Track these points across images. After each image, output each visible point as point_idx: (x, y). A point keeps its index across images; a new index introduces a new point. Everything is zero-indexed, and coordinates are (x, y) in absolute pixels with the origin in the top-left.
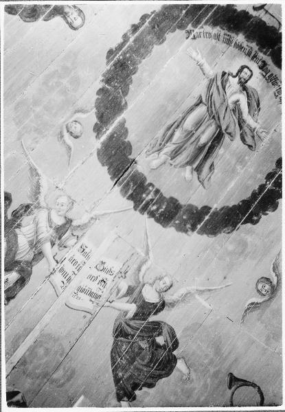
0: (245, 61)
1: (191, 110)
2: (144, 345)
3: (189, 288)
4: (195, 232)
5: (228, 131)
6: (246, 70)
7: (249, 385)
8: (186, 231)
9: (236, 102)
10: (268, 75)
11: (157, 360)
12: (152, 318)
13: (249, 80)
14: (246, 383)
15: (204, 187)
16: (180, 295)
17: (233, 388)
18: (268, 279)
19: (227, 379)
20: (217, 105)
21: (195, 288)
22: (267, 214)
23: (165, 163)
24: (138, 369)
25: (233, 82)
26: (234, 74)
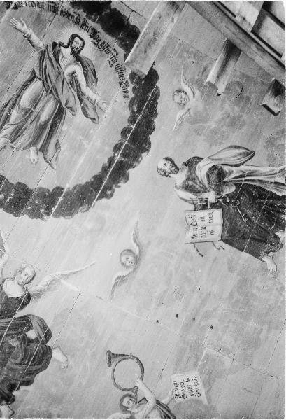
0: (74, 30)
1: (26, 86)
2: (14, 343)
3: (54, 275)
4: (51, 216)
5: (69, 105)
6: (77, 39)
7: (127, 359)
8: (40, 217)
9: (73, 74)
10: (100, 43)
11: (31, 355)
12: (19, 314)
13: (82, 49)
15: (53, 168)
16: (45, 283)
17: (113, 365)
18: (130, 251)
19: (106, 357)
20: (53, 79)
21: (60, 273)
22: (119, 187)
23: (5, 147)
24: (11, 369)
25: (66, 52)
26: (66, 44)
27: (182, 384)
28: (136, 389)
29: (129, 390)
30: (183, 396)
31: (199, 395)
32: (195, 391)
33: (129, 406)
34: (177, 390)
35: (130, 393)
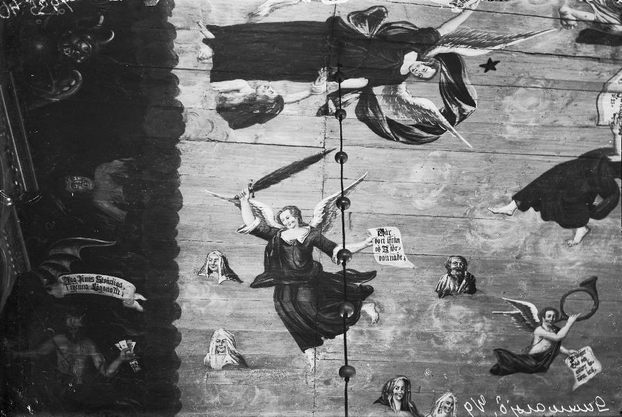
14: (594, 295)
17: (583, 288)
27: (585, 359)
28: (566, 318)
30: (573, 365)
31: (580, 379)
32: (582, 373)
33: (547, 318)
35: (560, 314)
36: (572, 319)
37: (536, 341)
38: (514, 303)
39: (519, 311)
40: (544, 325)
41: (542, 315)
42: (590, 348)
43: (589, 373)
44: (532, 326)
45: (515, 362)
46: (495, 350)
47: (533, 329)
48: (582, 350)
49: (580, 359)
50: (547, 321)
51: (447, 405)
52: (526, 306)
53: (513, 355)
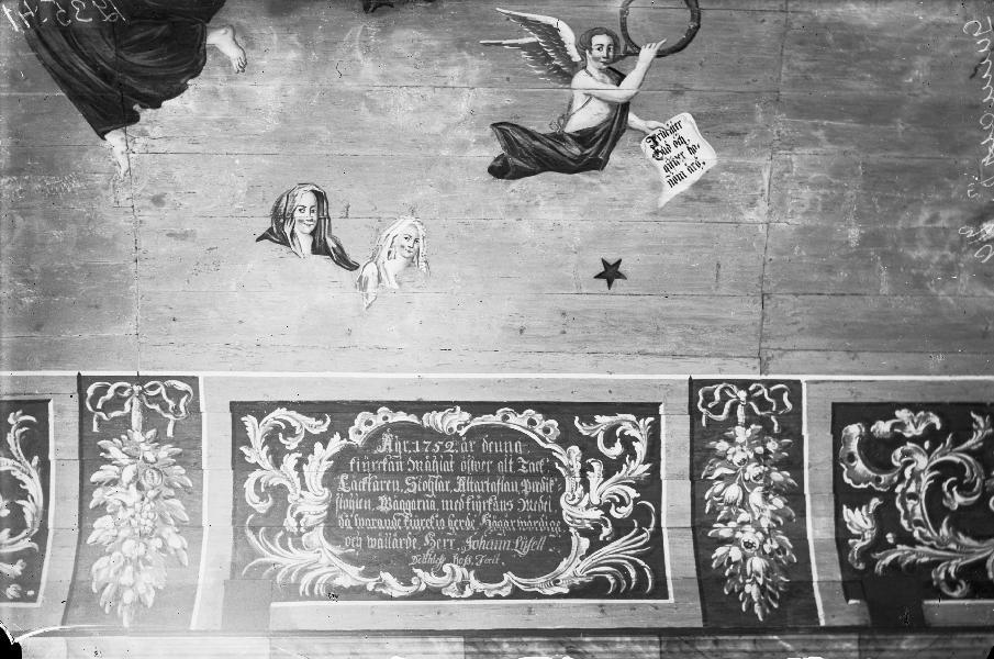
27: (680, 141)
28: (635, 51)
29: (627, 37)
30: (657, 152)
31: (673, 182)
33: (596, 53)
34: (665, 135)
35: (622, 43)
36: (647, 54)
37: (577, 104)
38: (524, 21)
39: (536, 38)
40: (592, 67)
41: (584, 46)
42: (689, 117)
43: (691, 170)
44: (566, 73)
45: (538, 151)
46: (494, 125)
47: (567, 77)
48: (674, 120)
49: (670, 139)
50: (596, 59)
51: (405, 242)
52: (550, 26)
53: (533, 136)
